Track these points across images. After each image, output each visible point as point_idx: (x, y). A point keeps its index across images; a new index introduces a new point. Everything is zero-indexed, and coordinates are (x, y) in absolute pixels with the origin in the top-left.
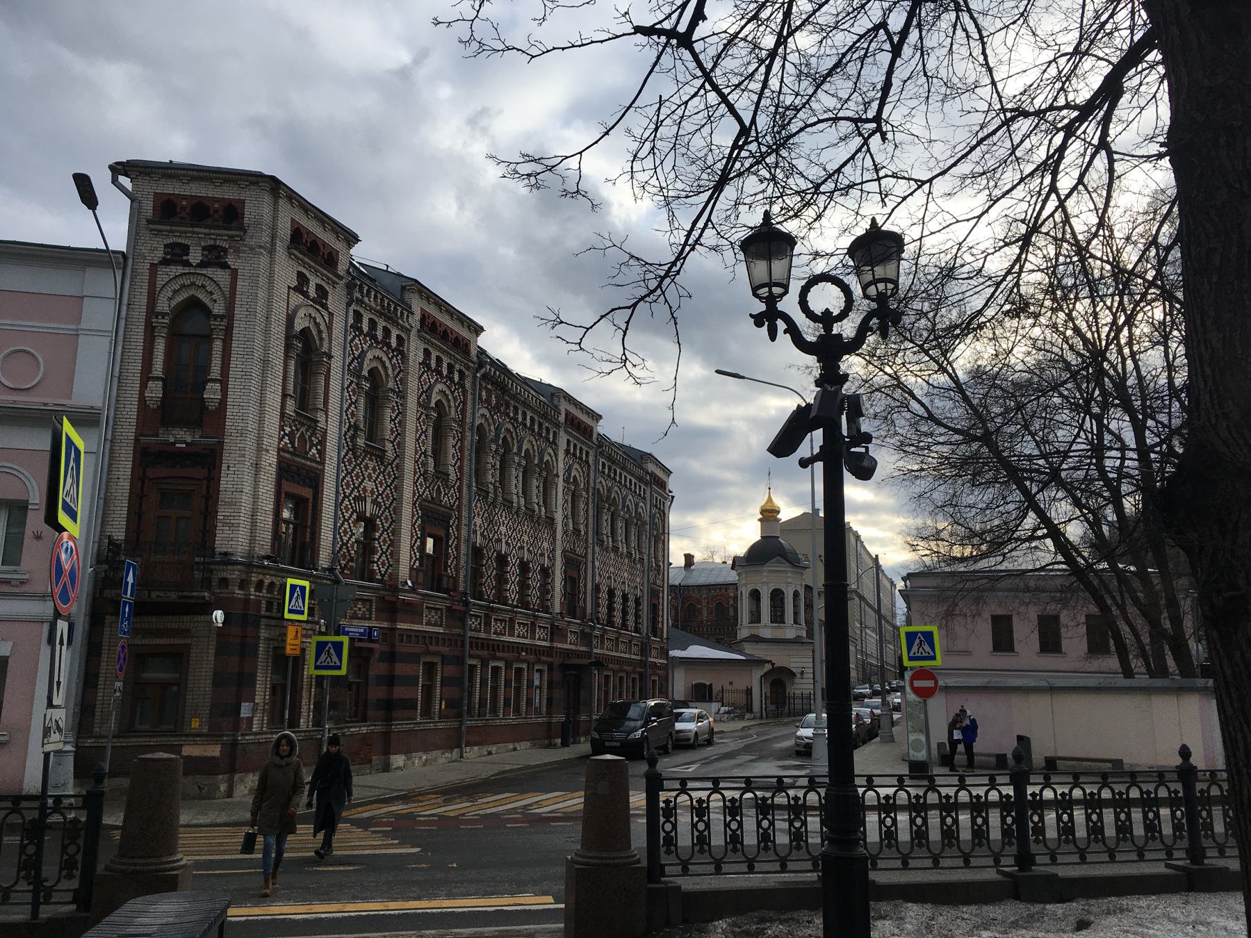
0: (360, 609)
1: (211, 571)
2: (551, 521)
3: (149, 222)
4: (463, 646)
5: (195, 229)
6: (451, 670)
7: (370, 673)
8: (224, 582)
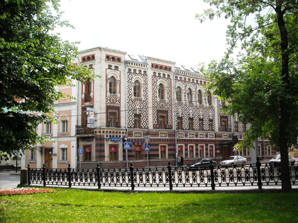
0: (138, 135)
2: (211, 108)
3: (80, 63)
5: (87, 62)
6: (172, 147)
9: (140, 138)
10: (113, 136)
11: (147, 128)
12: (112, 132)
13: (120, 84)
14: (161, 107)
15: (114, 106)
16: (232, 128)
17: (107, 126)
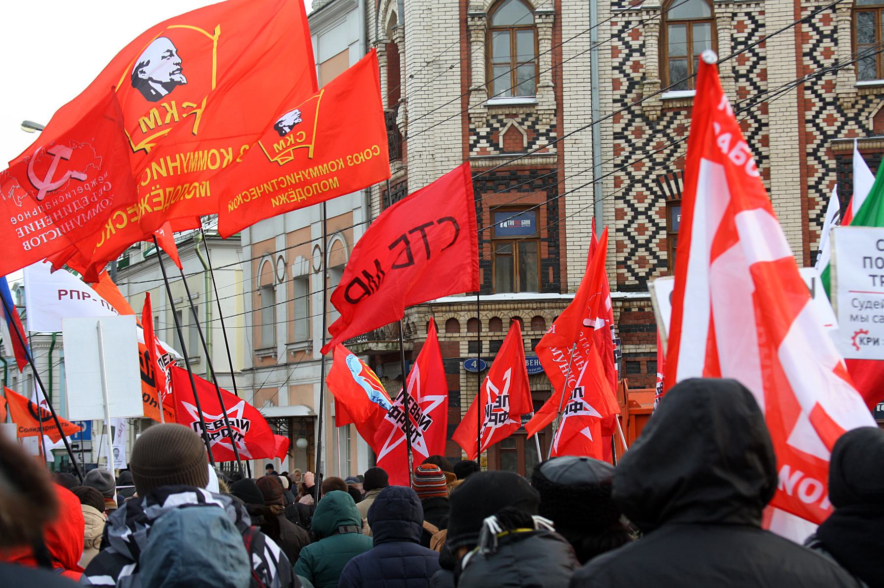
12: (506, 322)
13: (557, 26)
15: (522, 168)
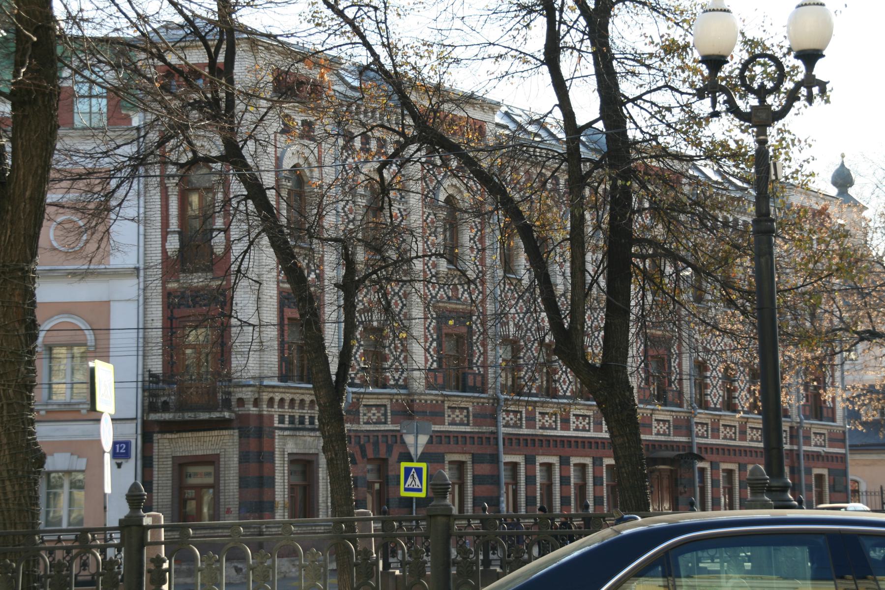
0: (374, 414)
1: (230, 393)
4: (497, 444)
6: (485, 469)
7: (390, 473)
8: (241, 402)
9: (382, 427)
10: (302, 420)
11: (405, 387)
12: (297, 402)
14: (449, 298)
16: (685, 390)
17: (283, 378)
